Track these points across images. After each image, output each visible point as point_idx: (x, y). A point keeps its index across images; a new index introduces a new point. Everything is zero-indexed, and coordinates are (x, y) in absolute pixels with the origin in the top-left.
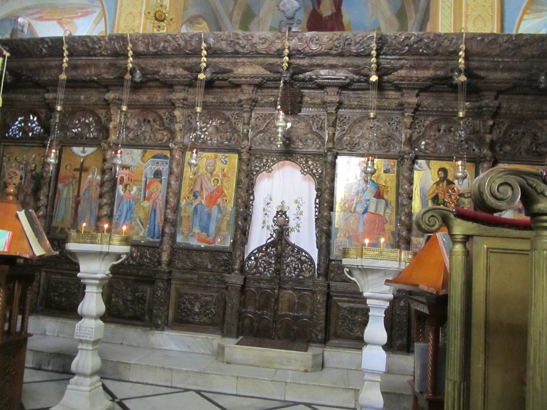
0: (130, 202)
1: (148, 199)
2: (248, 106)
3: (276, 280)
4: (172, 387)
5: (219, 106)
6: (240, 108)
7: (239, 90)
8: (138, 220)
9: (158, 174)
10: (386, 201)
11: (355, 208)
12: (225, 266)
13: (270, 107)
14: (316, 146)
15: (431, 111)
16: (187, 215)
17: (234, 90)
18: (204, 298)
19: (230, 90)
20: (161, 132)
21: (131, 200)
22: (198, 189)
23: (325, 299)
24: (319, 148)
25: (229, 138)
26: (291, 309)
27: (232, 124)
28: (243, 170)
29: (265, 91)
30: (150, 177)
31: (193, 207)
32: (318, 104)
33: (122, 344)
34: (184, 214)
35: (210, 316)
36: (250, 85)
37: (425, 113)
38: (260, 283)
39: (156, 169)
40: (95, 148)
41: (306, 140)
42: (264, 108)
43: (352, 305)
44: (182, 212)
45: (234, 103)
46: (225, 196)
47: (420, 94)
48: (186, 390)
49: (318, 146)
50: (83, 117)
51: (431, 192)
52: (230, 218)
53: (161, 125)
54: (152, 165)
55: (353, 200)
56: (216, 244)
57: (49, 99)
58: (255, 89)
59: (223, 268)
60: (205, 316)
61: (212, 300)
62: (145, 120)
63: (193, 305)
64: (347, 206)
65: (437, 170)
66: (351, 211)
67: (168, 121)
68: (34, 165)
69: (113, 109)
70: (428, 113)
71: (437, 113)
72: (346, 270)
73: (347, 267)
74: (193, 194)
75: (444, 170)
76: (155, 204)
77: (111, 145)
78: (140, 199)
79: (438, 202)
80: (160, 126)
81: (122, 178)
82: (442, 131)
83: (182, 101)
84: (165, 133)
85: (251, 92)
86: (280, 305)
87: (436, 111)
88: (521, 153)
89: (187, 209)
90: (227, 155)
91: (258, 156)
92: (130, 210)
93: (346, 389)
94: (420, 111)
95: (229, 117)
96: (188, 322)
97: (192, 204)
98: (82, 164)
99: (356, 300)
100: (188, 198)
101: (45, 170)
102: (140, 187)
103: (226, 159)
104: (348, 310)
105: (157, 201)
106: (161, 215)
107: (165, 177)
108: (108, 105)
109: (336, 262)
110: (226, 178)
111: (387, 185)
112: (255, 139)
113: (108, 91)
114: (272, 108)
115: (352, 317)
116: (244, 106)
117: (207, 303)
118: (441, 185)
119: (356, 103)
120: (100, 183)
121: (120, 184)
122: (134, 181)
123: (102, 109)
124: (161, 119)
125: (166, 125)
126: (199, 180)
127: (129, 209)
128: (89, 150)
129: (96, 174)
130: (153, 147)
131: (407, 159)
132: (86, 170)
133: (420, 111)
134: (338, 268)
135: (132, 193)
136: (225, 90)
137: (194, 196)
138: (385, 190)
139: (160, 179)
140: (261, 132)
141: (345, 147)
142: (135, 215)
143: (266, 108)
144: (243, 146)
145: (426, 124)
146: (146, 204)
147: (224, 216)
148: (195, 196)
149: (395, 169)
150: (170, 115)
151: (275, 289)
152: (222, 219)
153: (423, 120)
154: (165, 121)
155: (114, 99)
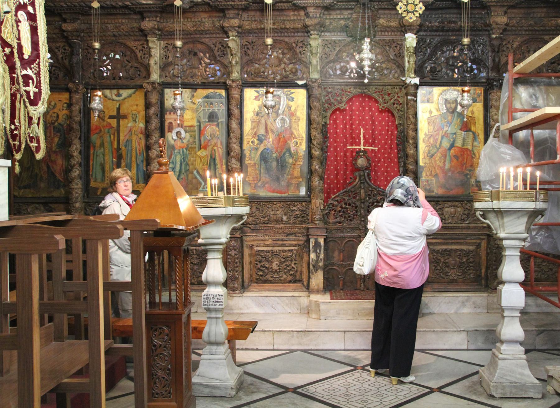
0: (183, 152)
1: (205, 148)
2: (316, 32)
3: (360, 227)
4: (274, 350)
5: (281, 32)
6: (306, 34)
7: (302, 13)
8: (195, 172)
9: (212, 117)
10: (474, 133)
11: (441, 142)
12: (303, 217)
13: (340, 32)
14: (394, 76)
15: (520, 30)
16: (252, 163)
17: (296, 13)
18: (283, 254)
19: (292, 13)
20: (212, 66)
21: (185, 150)
22: (262, 131)
25: (294, 70)
27: (296, 54)
28: (315, 107)
29: (333, 13)
30: (204, 120)
31: (259, 152)
32: (396, 27)
33: (196, 312)
34: (249, 162)
35: (292, 273)
36: (317, 7)
37: (513, 33)
38: (342, 232)
39: (210, 111)
40: (133, 90)
41: (383, 69)
42: (333, 34)
43: (444, 247)
44: (247, 159)
45: (298, 29)
46: (295, 138)
47: (509, 11)
48: (292, 351)
49: (396, 75)
50: (112, 51)
52: (303, 163)
53: (211, 58)
54: (205, 107)
55: (438, 134)
56: (290, 193)
57: (68, 31)
58: (323, 11)
59: (299, 219)
60: (285, 273)
61: (292, 255)
62: (190, 52)
63: (270, 262)
64: (431, 140)
66: (436, 147)
67: (220, 53)
68: (55, 115)
69: (152, 41)
70: (517, 32)
71: (527, 33)
72: (478, 213)
73: (481, 211)
74: (257, 138)
76: (213, 151)
77: (157, 85)
78: (195, 147)
80: (209, 59)
81: (171, 123)
83: (237, 28)
84: (217, 68)
85: (318, 16)
87: (526, 31)
89: (253, 156)
90: (293, 90)
91: (329, 90)
92: (184, 161)
93: (458, 331)
94: (509, 31)
95: (292, 45)
96: (266, 282)
97: (257, 149)
98: (118, 109)
100: (252, 142)
101: (74, 120)
102: (193, 133)
103: (292, 95)
104: (441, 253)
105: (215, 148)
106: (222, 165)
107: (222, 119)
108: (146, 36)
110: (294, 118)
111: (474, 116)
112: (325, 70)
113: (143, 18)
114: (342, 34)
116: (312, 32)
117: (286, 258)
119: (437, 24)
120: (144, 132)
121: (169, 132)
122: (186, 126)
123: (135, 40)
124: (211, 50)
125: (218, 58)
126: (263, 121)
127: (184, 159)
128: (125, 93)
129: (137, 120)
130: (205, 85)
132: (125, 117)
133: (509, 31)
135: (185, 141)
136: (285, 13)
137: (258, 140)
138: (472, 121)
139: (215, 123)
140: (334, 61)
142: (191, 167)
143: (336, 34)
144: (314, 80)
145: (515, 46)
146: (202, 153)
147: (296, 161)
148: (261, 141)
149: (482, 98)
150: (222, 46)
152: (294, 164)
153: (511, 41)
154: (217, 54)
155: (154, 28)
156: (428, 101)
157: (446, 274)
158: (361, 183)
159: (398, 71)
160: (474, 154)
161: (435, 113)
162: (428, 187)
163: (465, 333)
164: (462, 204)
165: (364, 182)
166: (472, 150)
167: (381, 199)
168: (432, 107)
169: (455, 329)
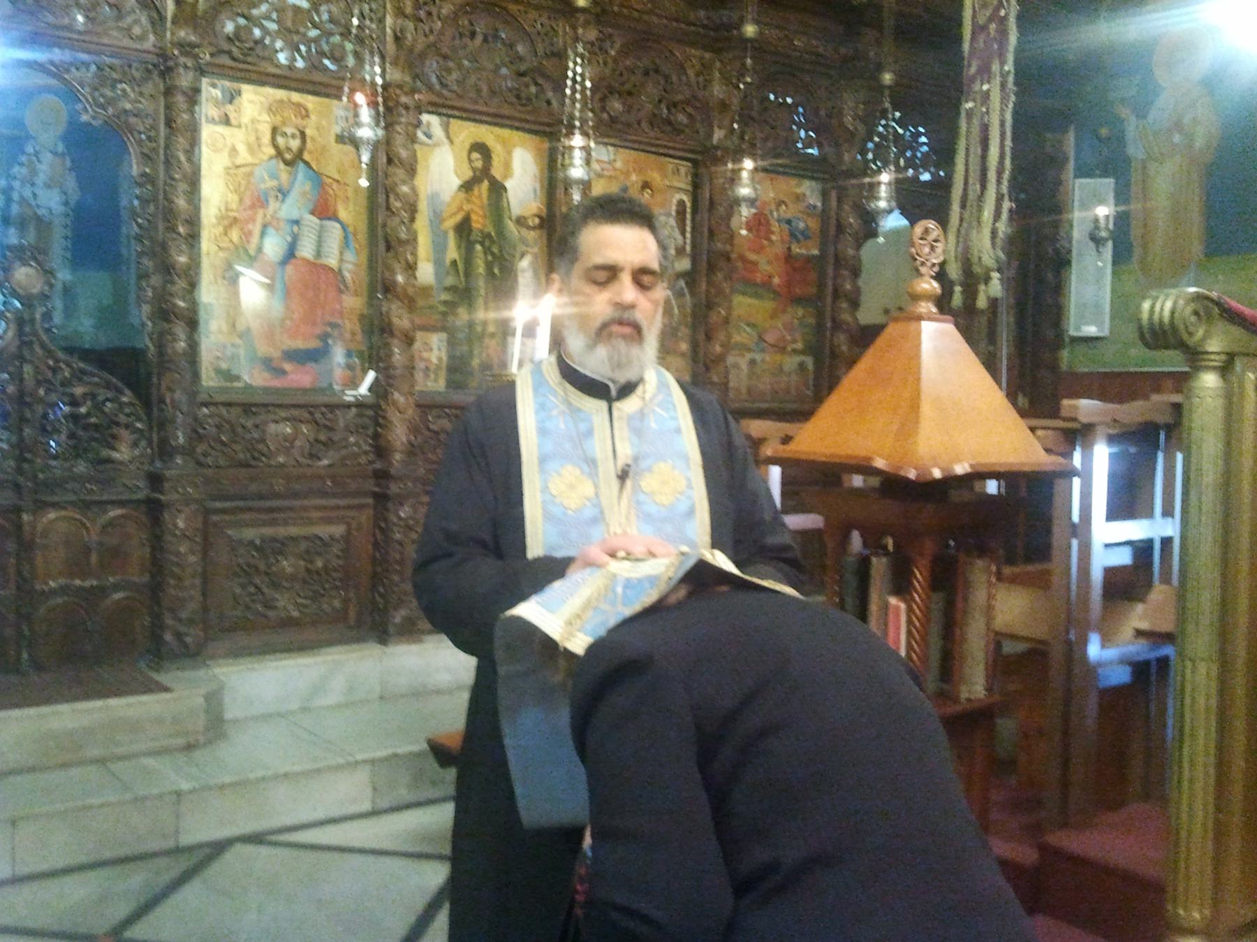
23: (200, 526)
24: (142, 38)
26: (77, 565)
43: (268, 531)
49: (137, 31)
51: (454, 208)
55: (253, 220)
64: (235, 235)
65: (467, 146)
75: (481, 148)
79: (469, 235)
82: (479, 39)
86: (39, 561)
88: (639, 123)
99: (276, 515)
104: (258, 549)
109: (212, 408)
115: (269, 566)
118: (476, 191)
131: (407, 108)
134: (218, 427)
141: (226, 46)
151: (18, 510)
156: (226, 121)
157: (269, 605)
158: (23, 343)
159: (144, 20)
160: (344, 282)
161: (244, 156)
162: (224, 366)
163: (368, 767)
164: (311, 413)
165: (31, 343)
166: (340, 270)
167: (85, 394)
168: (237, 137)
169: (341, 761)
